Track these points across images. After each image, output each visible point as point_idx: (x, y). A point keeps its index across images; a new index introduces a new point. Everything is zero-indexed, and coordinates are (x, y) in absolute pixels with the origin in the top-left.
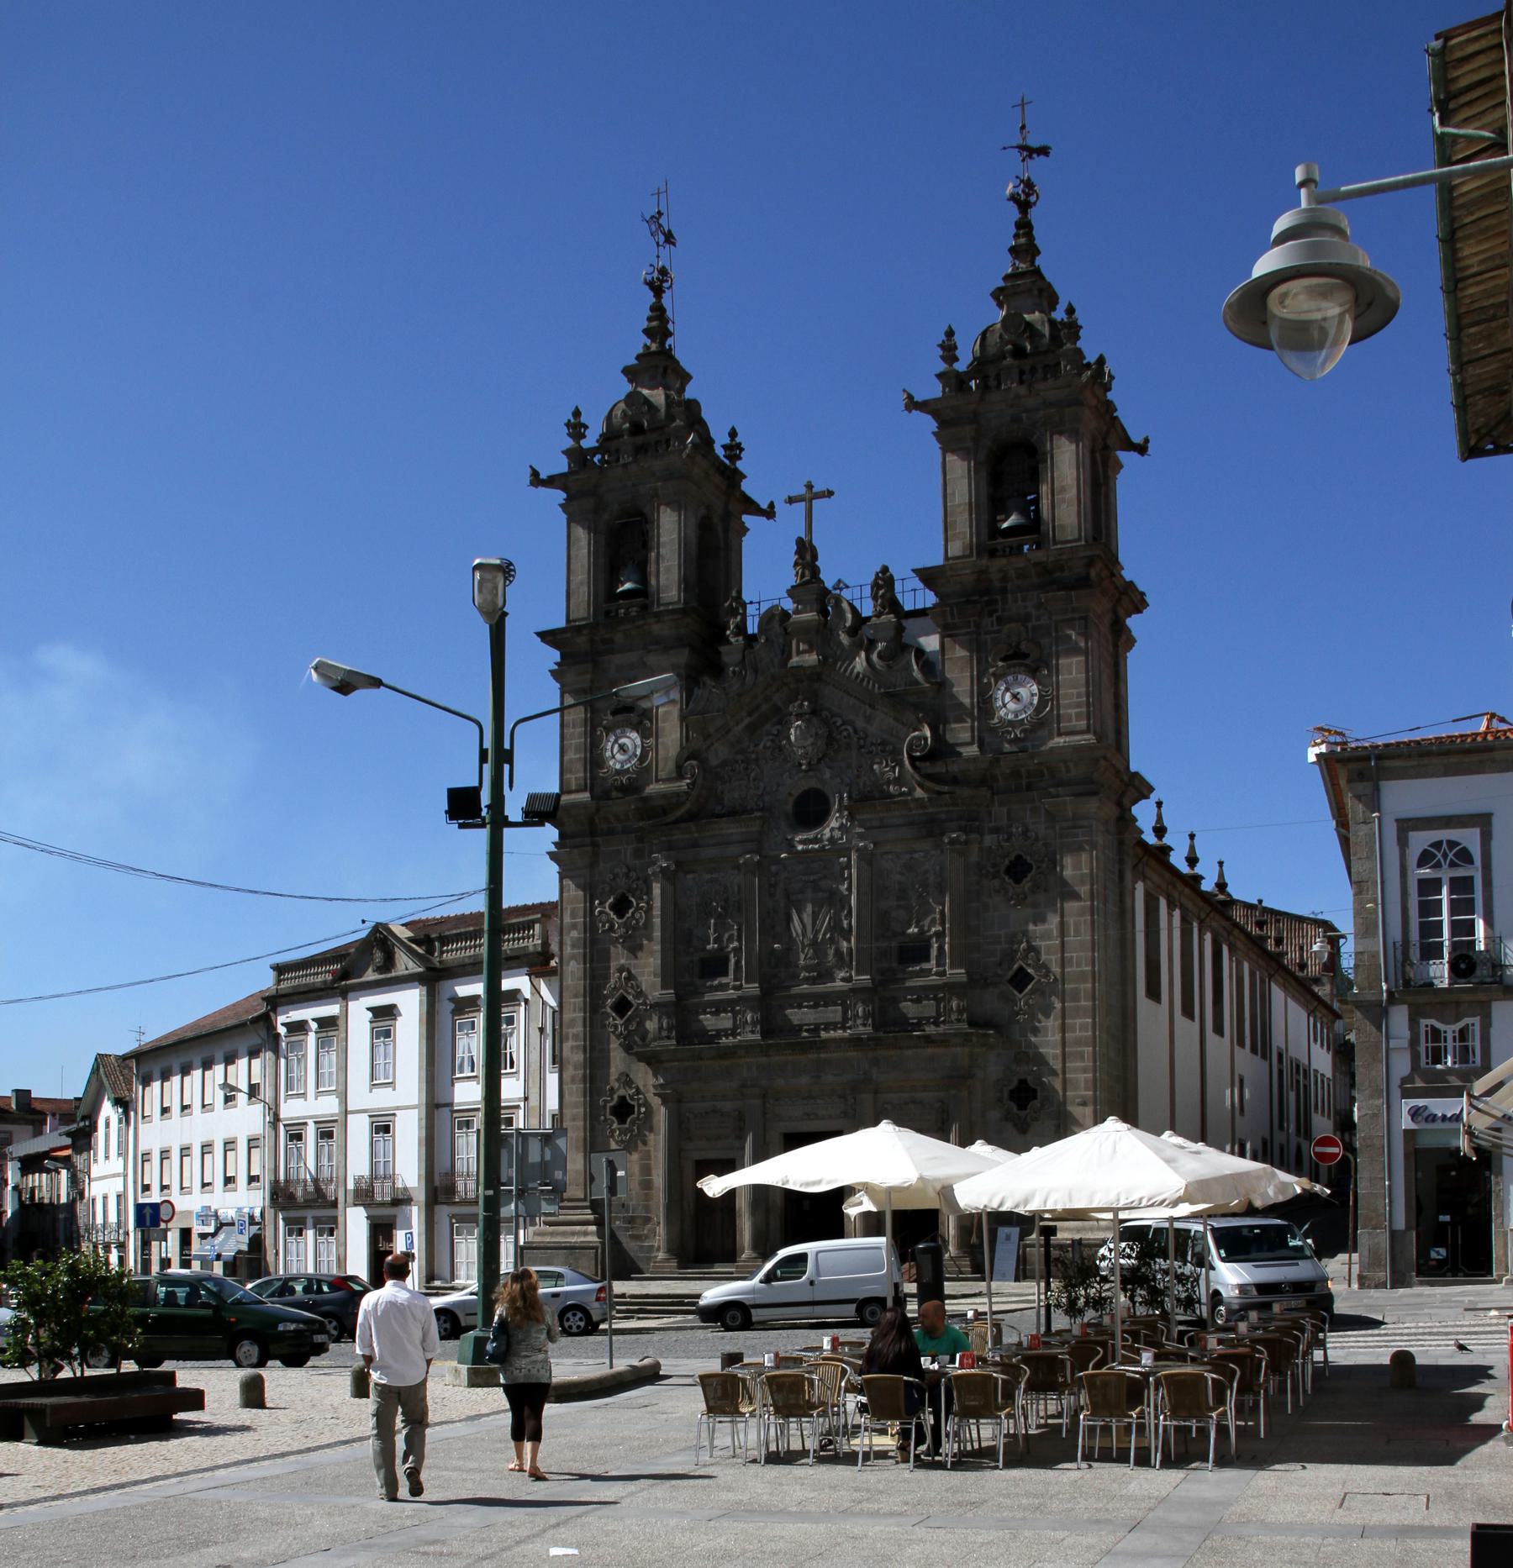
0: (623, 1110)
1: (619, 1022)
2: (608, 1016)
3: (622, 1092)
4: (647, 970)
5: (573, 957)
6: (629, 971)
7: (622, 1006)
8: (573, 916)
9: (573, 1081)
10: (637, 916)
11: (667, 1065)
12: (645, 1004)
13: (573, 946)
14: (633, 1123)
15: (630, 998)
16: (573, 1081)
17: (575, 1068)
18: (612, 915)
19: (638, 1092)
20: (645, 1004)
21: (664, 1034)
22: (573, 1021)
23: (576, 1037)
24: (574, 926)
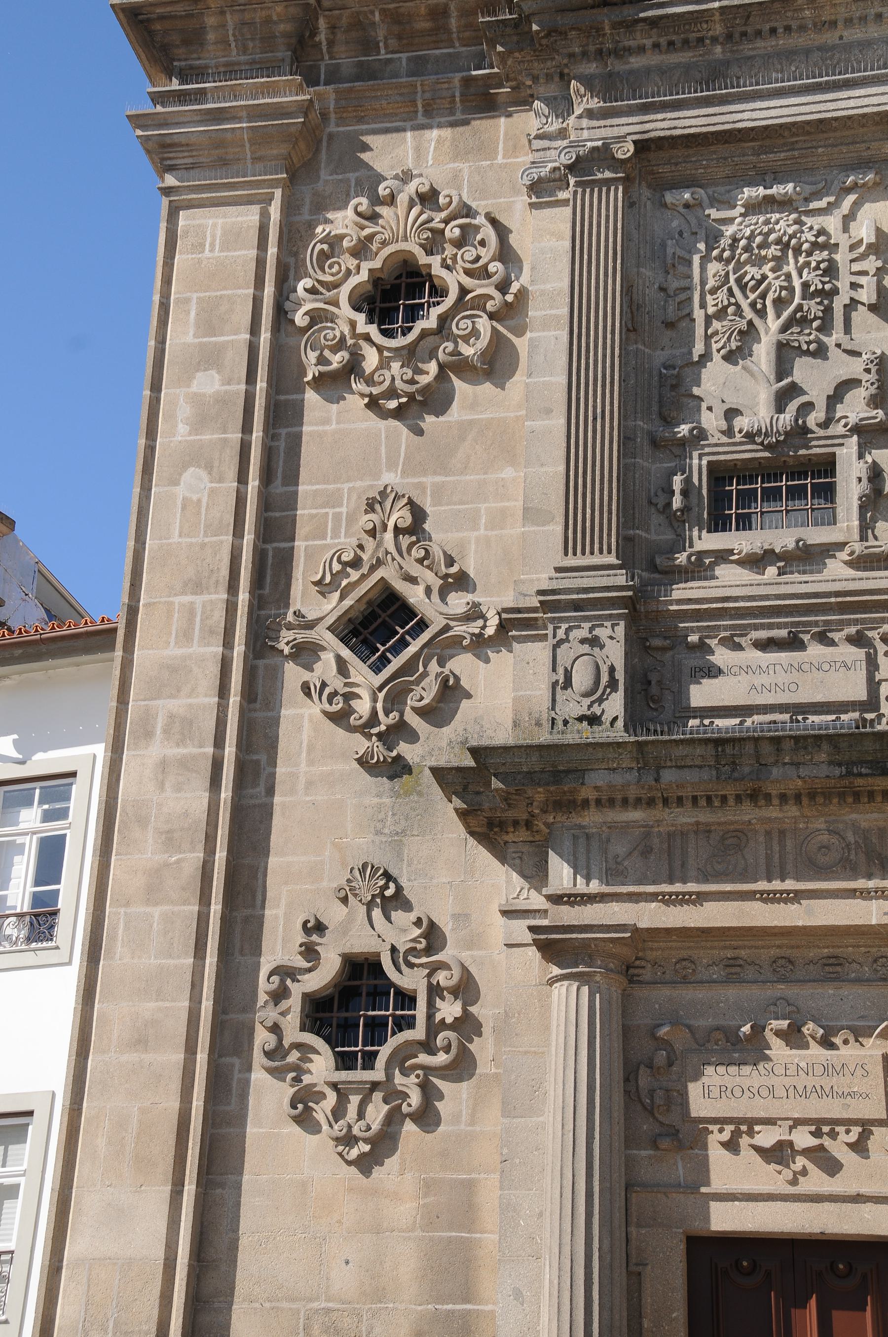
0: (355, 1006)
1: (363, 676)
2: (306, 653)
3: (362, 942)
4: (497, 488)
5: (194, 456)
6: (418, 514)
7: (379, 623)
8: (209, 323)
9: (153, 892)
10: (460, 326)
11: (591, 819)
12: (474, 613)
13: (200, 422)
14: (399, 1059)
15: (415, 595)
16: (153, 892)
17: (169, 841)
18: (363, 325)
19: (433, 937)
20: (474, 613)
21: (572, 706)
22: (174, 676)
23: (178, 729)
24: (209, 358)
